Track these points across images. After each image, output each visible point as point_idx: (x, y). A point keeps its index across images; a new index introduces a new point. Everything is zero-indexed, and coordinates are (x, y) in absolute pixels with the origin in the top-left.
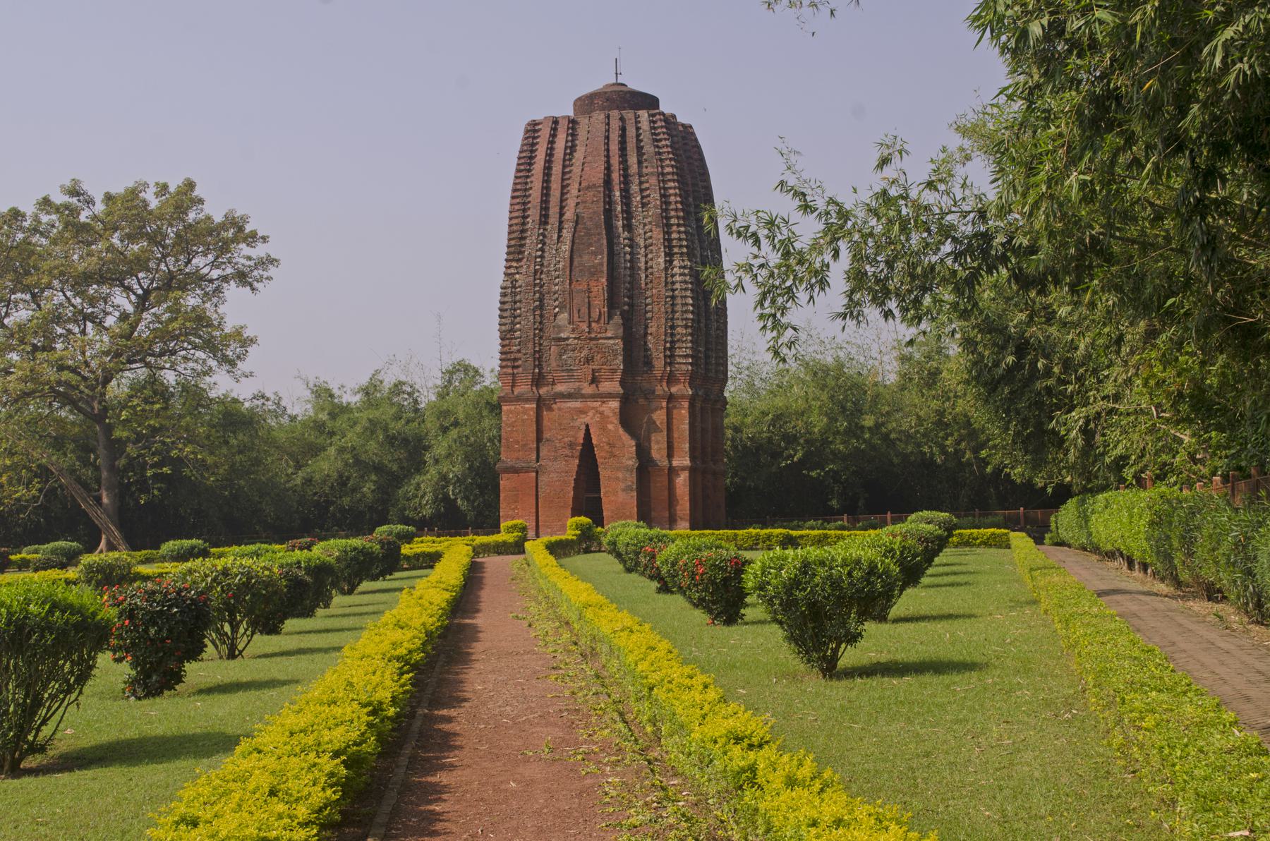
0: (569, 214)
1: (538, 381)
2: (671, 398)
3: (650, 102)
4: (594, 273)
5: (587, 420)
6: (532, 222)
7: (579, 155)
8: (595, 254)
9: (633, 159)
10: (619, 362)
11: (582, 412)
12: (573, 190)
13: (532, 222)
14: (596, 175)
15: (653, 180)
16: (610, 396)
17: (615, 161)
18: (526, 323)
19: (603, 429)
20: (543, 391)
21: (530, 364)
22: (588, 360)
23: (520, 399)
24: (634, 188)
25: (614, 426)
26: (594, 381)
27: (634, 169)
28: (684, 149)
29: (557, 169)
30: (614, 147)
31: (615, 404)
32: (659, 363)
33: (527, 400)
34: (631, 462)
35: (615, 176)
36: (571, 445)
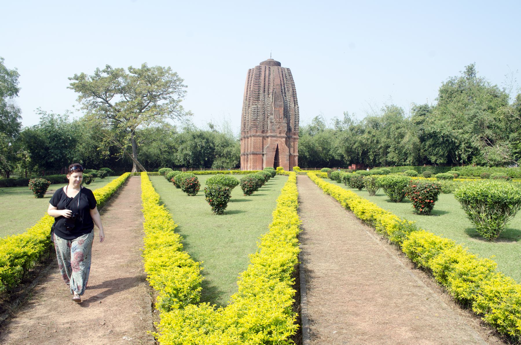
0: (271, 91)
1: (263, 132)
2: (295, 139)
3: (279, 64)
4: (280, 107)
5: (277, 143)
6: (261, 92)
7: (271, 76)
8: (280, 102)
9: (285, 79)
10: (286, 129)
11: (276, 141)
12: (272, 85)
13: (261, 92)
14: (278, 81)
15: (290, 85)
16: (284, 137)
17: (282, 79)
18: (261, 117)
19: (282, 145)
20: (264, 135)
21: (262, 127)
22: (279, 128)
23: (259, 136)
24: (286, 86)
25: (284, 144)
26: (280, 133)
27: (285, 82)
28: (287, 77)
29: (267, 79)
30: (281, 76)
31: (284, 139)
32: (293, 130)
33: (260, 137)
34: (288, 154)
35: (282, 83)
36: (274, 149)
